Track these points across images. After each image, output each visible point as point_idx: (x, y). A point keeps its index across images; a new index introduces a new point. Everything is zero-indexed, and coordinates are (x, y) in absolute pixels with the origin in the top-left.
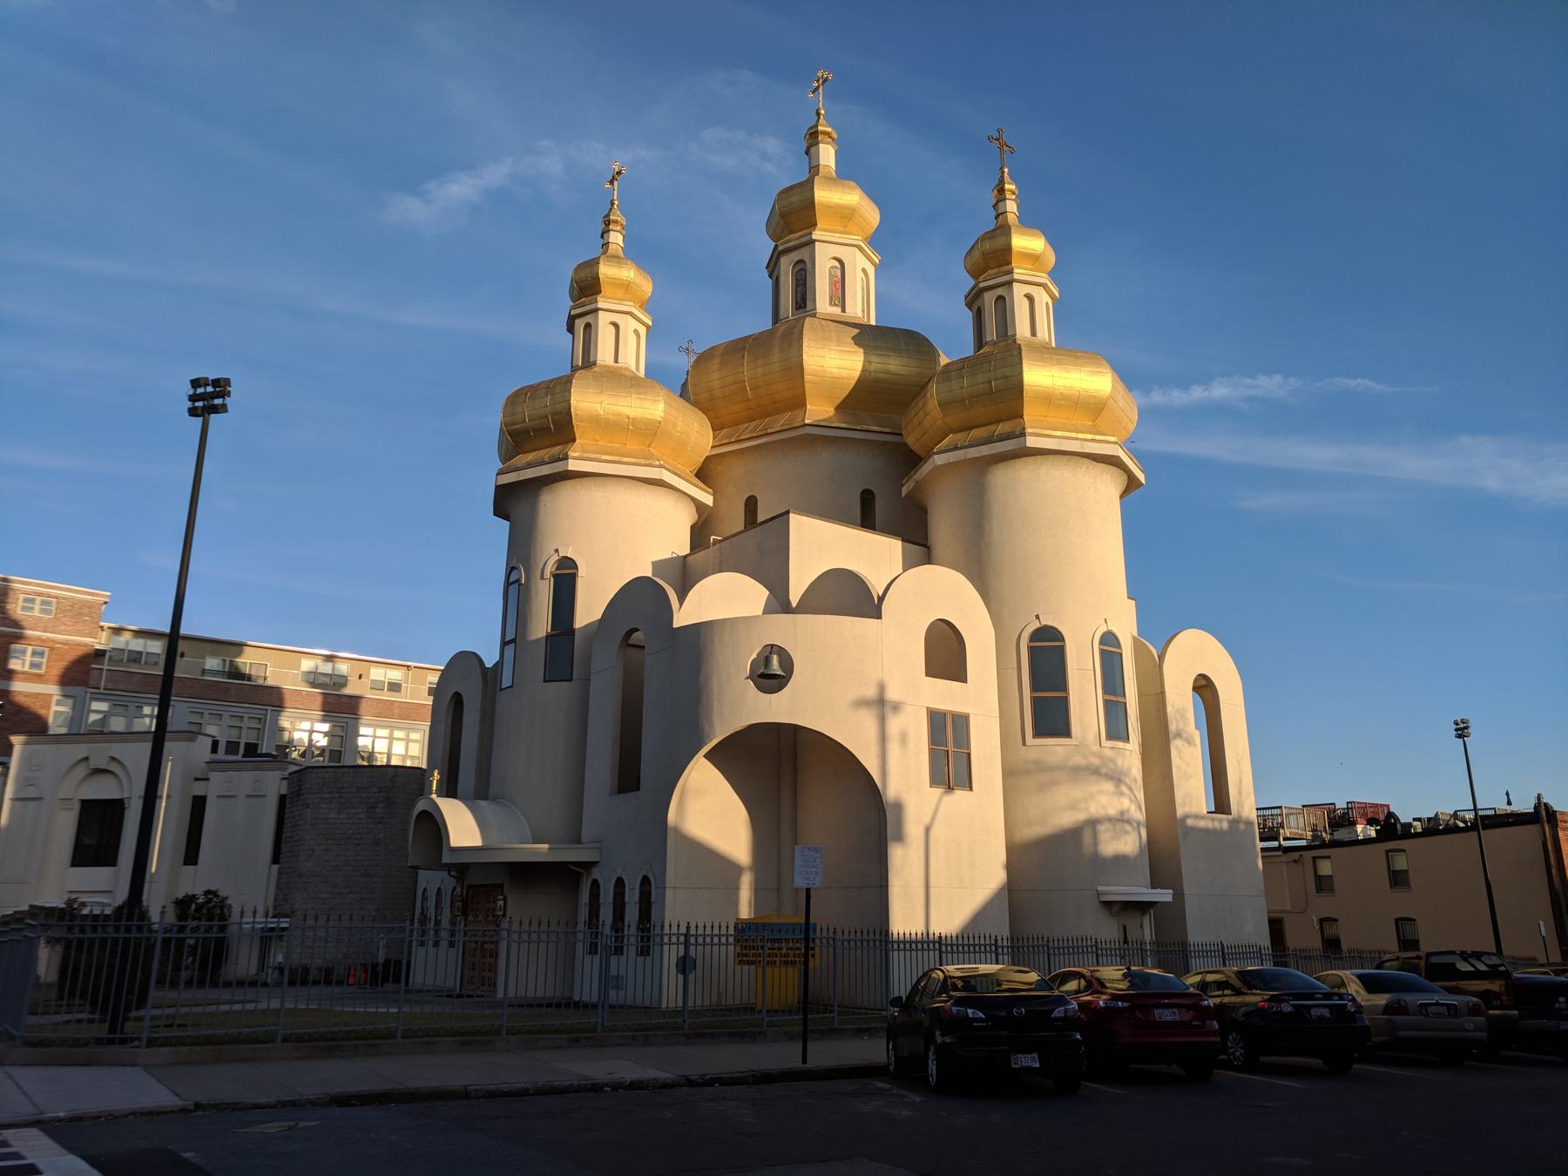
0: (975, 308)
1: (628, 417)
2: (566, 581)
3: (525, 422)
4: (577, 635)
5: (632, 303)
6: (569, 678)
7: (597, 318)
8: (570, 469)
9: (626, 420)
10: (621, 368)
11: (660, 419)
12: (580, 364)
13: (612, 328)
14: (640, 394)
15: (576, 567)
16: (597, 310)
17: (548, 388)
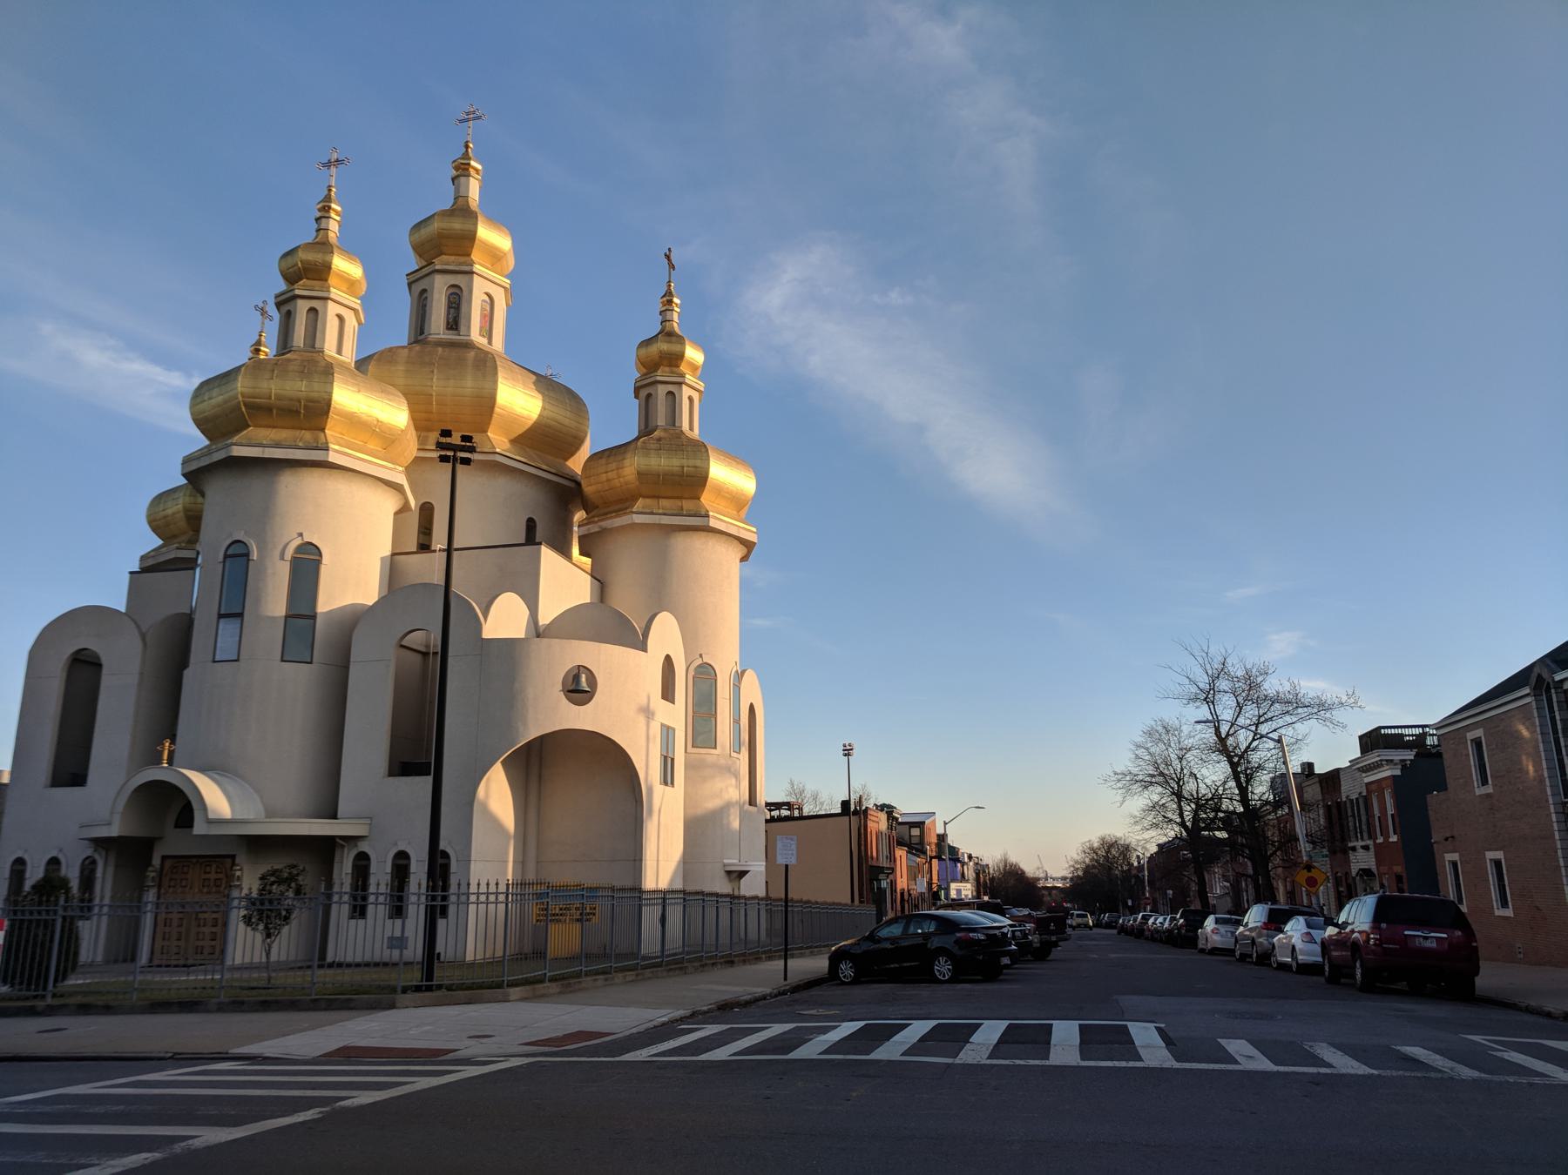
0: (643, 393)
1: (378, 421)
2: (307, 564)
3: (270, 398)
4: (319, 620)
5: (359, 302)
6: (309, 661)
7: (326, 308)
8: (330, 460)
9: (375, 423)
10: (345, 363)
11: (403, 428)
12: (302, 346)
13: (336, 319)
14: (390, 400)
15: (320, 554)
16: (327, 299)
17: (276, 364)
